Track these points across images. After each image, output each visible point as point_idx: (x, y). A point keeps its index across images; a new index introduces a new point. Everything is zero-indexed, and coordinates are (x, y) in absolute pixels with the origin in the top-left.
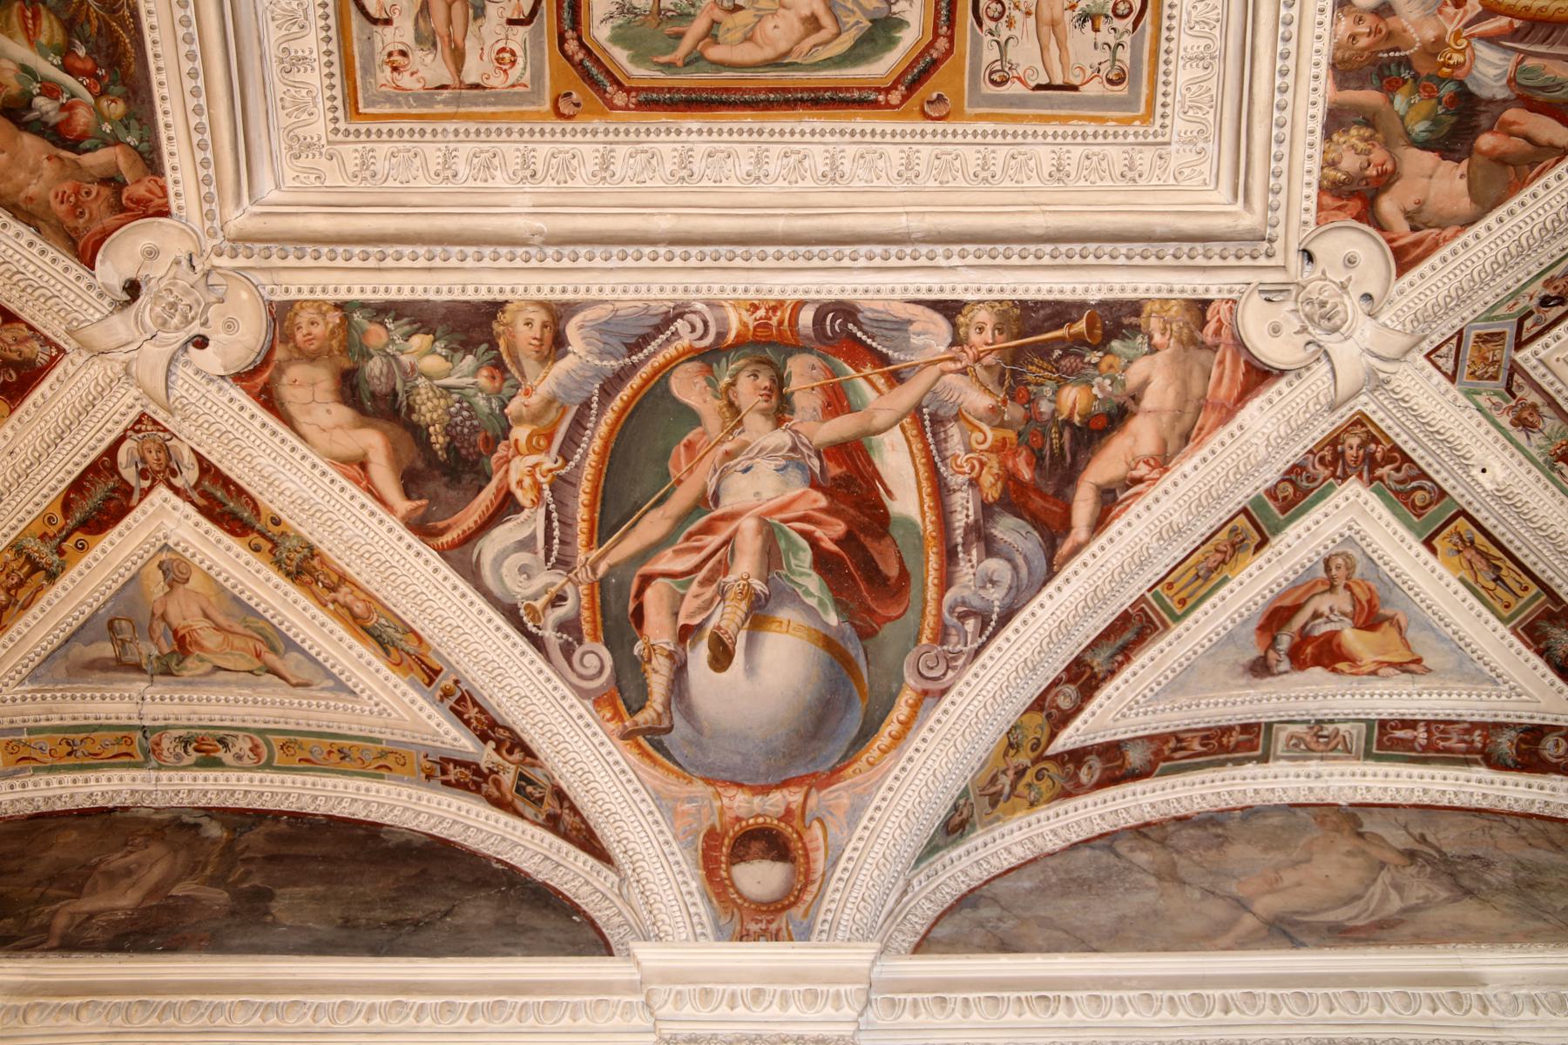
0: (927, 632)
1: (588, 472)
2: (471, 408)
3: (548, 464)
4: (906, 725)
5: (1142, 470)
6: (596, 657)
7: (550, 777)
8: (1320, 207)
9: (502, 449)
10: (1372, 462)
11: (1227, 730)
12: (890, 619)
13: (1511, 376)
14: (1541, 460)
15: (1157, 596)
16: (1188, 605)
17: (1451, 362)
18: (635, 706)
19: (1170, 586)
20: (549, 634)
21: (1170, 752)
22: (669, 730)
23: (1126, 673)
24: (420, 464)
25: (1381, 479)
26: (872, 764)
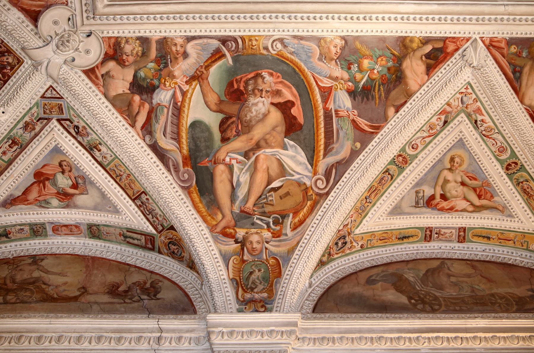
8: (110, 38)
13: (46, 119)
17: (50, 96)
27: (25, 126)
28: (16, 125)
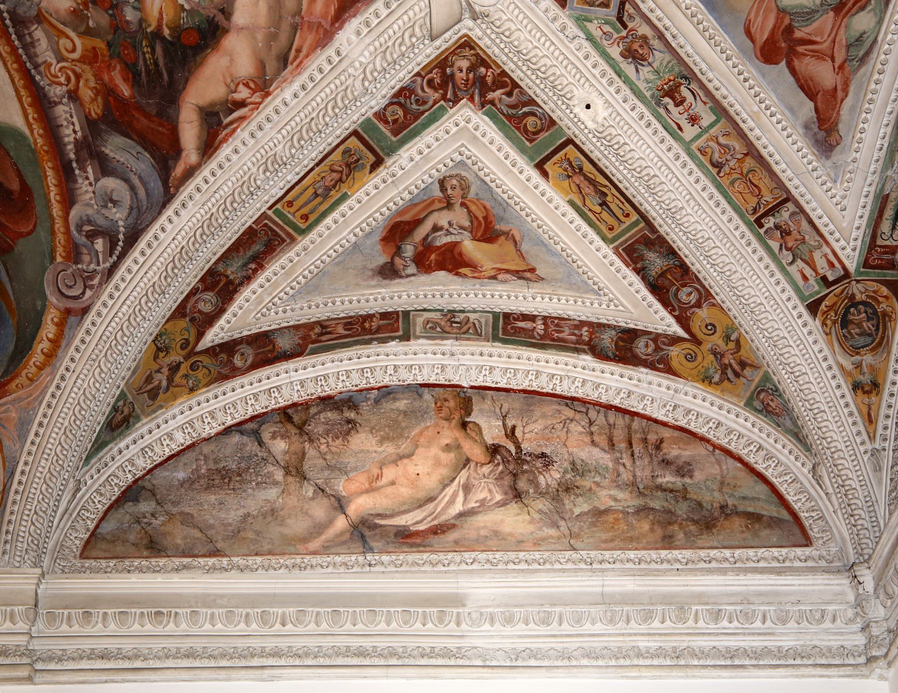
0: (60, 250)
5: (243, 93)
10: (483, 87)
11: (370, 317)
12: (22, 235)
14: (648, 94)
15: (278, 213)
16: (310, 222)
19: (290, 204)
21: (315, 338)
23: (261, 279)
25: (492, 102)
27: (634, 58)
28: (627, 81)
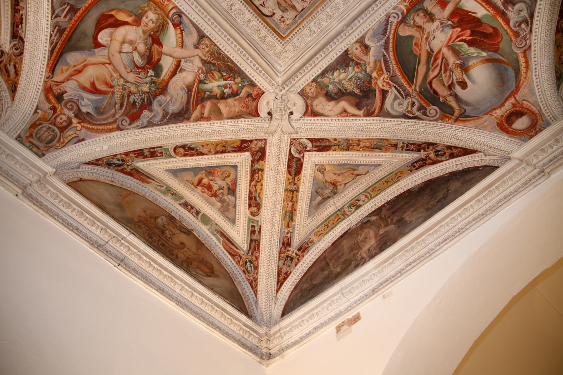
1: (397, 70)
2: (359, 78)
3: (386, 76)
4: (527, 62)
6: (433, 110)
7: (444, 145)
9: (373, 82)
18: (452, 113)
20: (417, 114)
22: (465, 111)
24: (357, 100)
26: (526, 78)
